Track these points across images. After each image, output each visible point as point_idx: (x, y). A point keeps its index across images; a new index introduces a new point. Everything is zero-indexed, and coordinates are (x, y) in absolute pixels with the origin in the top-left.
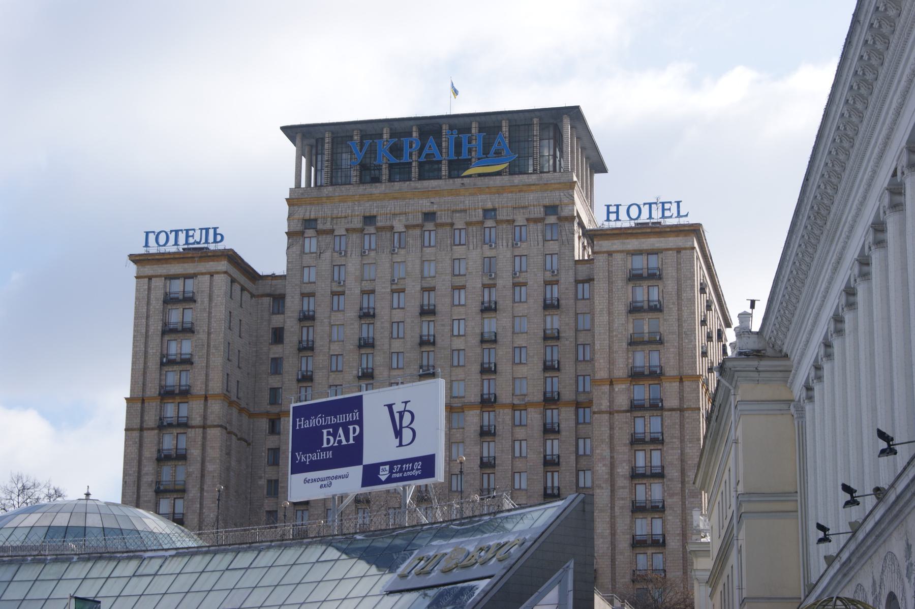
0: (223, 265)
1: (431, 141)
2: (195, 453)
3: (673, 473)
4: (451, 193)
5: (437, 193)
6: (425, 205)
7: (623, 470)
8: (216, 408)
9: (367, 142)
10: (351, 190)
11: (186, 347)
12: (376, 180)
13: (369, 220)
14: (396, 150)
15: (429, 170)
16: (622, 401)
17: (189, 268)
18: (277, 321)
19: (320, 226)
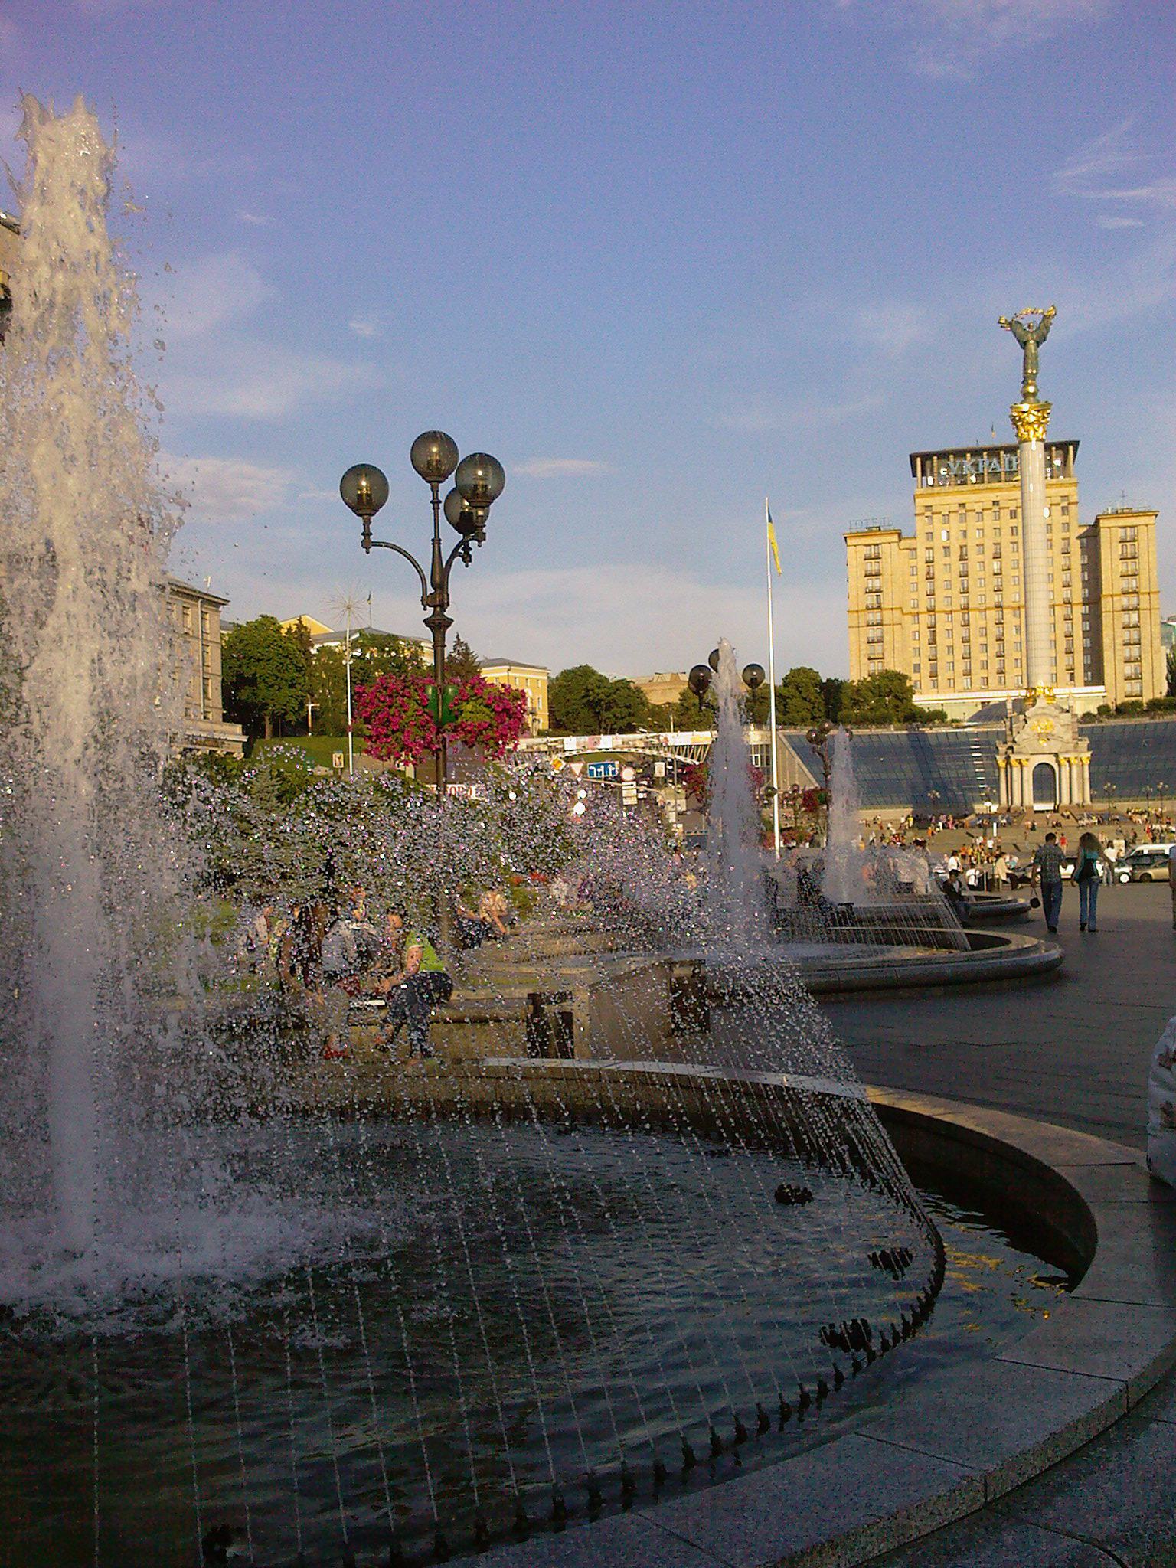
0: (895, 538)
1: (995, 460)
2: (886, 638)
3: (1145, 641)
4: (1008, 489)
5: (1000, 489)
6: (993, 496)
7: (1119, 641)
8: (897, 613)
9: (958, 462)
10: (947, 489)
11: (876, 583)
12: (963, 483)
13: (962, 505)
14: (976, 465)
15: (995, 475)
16: (1118, 607)
17: (876, 540)
18: (913, 562)
19: (934, 509)
